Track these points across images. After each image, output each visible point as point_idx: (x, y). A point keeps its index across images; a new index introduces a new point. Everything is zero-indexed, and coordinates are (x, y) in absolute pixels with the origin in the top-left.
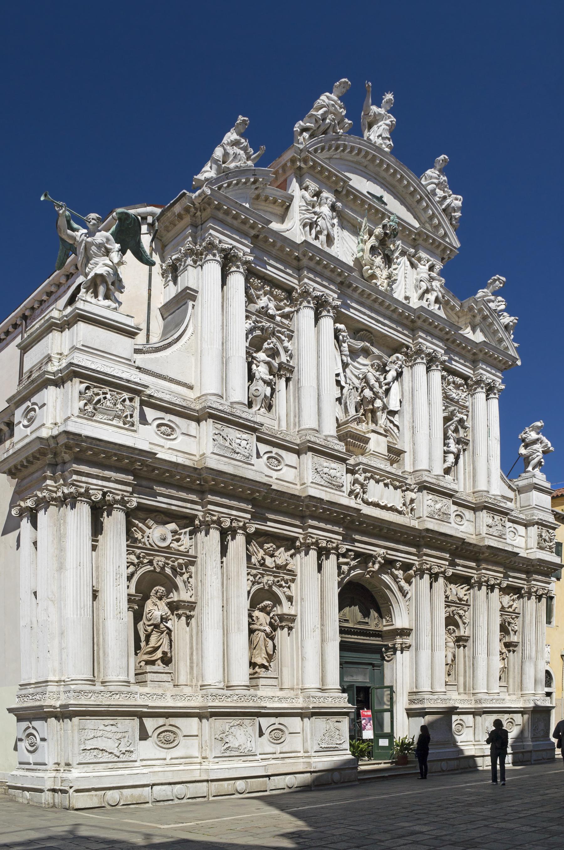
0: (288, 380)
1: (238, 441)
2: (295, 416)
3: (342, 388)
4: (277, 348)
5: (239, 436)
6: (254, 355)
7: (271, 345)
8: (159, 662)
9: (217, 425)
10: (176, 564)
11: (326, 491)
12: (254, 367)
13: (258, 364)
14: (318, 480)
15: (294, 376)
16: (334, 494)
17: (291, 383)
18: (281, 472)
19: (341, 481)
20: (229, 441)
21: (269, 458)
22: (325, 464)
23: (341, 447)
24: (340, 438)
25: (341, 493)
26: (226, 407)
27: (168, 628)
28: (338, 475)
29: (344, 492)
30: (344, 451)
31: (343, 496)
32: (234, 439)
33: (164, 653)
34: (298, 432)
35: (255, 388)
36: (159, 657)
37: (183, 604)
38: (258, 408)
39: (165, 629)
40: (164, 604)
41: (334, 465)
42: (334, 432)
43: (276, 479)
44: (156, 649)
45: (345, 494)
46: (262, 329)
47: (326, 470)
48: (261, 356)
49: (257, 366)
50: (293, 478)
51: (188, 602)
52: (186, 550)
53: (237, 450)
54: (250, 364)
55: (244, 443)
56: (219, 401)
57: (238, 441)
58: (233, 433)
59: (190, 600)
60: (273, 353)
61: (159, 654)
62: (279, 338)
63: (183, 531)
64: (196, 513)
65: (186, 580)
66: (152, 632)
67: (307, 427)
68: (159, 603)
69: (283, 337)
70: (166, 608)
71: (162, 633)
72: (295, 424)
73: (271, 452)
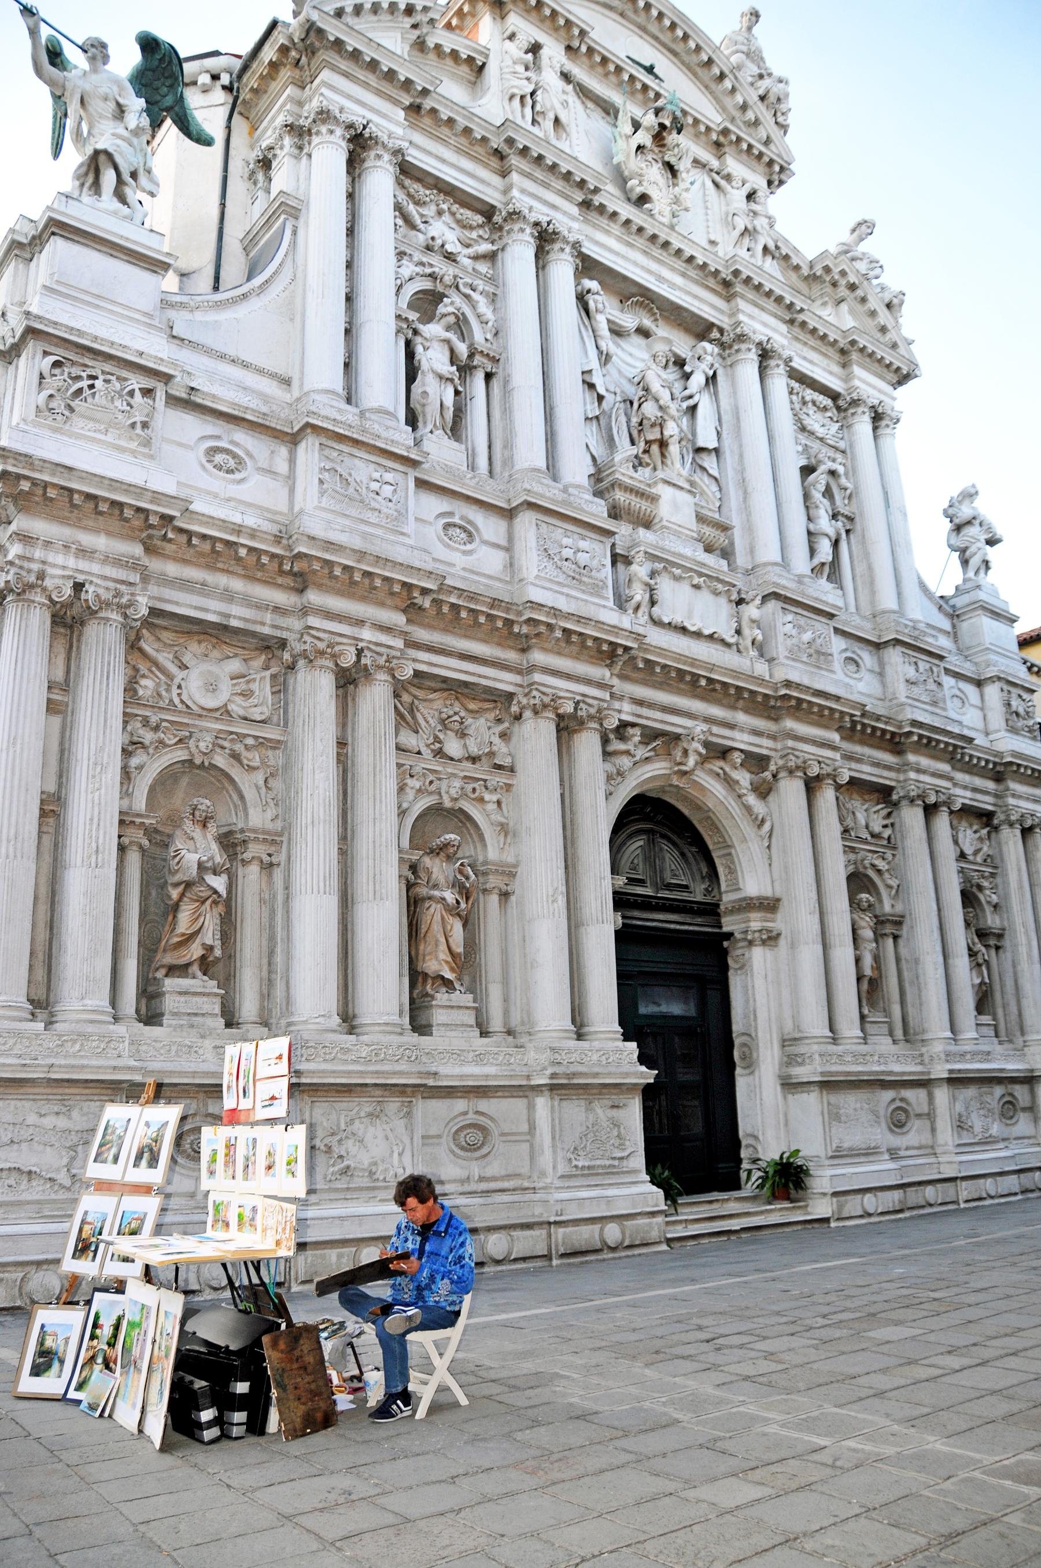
0: (488, 377)
1: (375, 486)
2: (505, 447)
3: (600, 398)
4: (463, 314)
5: (376, 475)
6: (421, 327)
7: (451, 309)
8: (195, 968)
9: (327, 452)
10: (239, 747)
11: (567, 595)
12: (419, 349)
13: (427, 344)
14: (551, 571)
15: (499, 370)
16: (586, 601)
17: (495, 383)
18: (475, 556)
19: (602, 575)
20: (353, 483)
21: (447, 526)
22: (566, 541)
23: (597, 511)
24: (598, 494)
25: (603, 602)
26: (350, 416)
27: (216, 892)
28: (595, 563)
29: (607, 599)
30: (606, 515)
31: (604, 606)
32: (365, 481)
33: (210, 949)
34: (510, 476)
35: (420, 391)
36: (195, 957)
37: (252, 835)
38: (428, 429)
39: (210, 893)
40: (210, 837)
41: (583, 544)
42: (585, 481)
43: (464, 569)
44: (190, 938)
45: (611, 603)
46: (432, 276)
47: (567, 553)
48: (433, 330)
49: (426, 349)
50: (501, 567)
51: (268, 833)
52: (263, 717)
53: (374, 504)
54: (408, 344)
55: (387, 490)
56: (335, 403)
57: (375, 486)
58: (362, 469)
59: (270, 826)
60: (460, 326)
61: (195, 951)
62: (467, 297)
63: (258, 676)
64: (284, 635)
65: (261, 783)
66: (180, 899)
67: (526, 465)
68: (197, 833)
69: (475, 296)
70: (215, 847)
71: (203, 902)
72: (505, 463)
73: (451, 514)
